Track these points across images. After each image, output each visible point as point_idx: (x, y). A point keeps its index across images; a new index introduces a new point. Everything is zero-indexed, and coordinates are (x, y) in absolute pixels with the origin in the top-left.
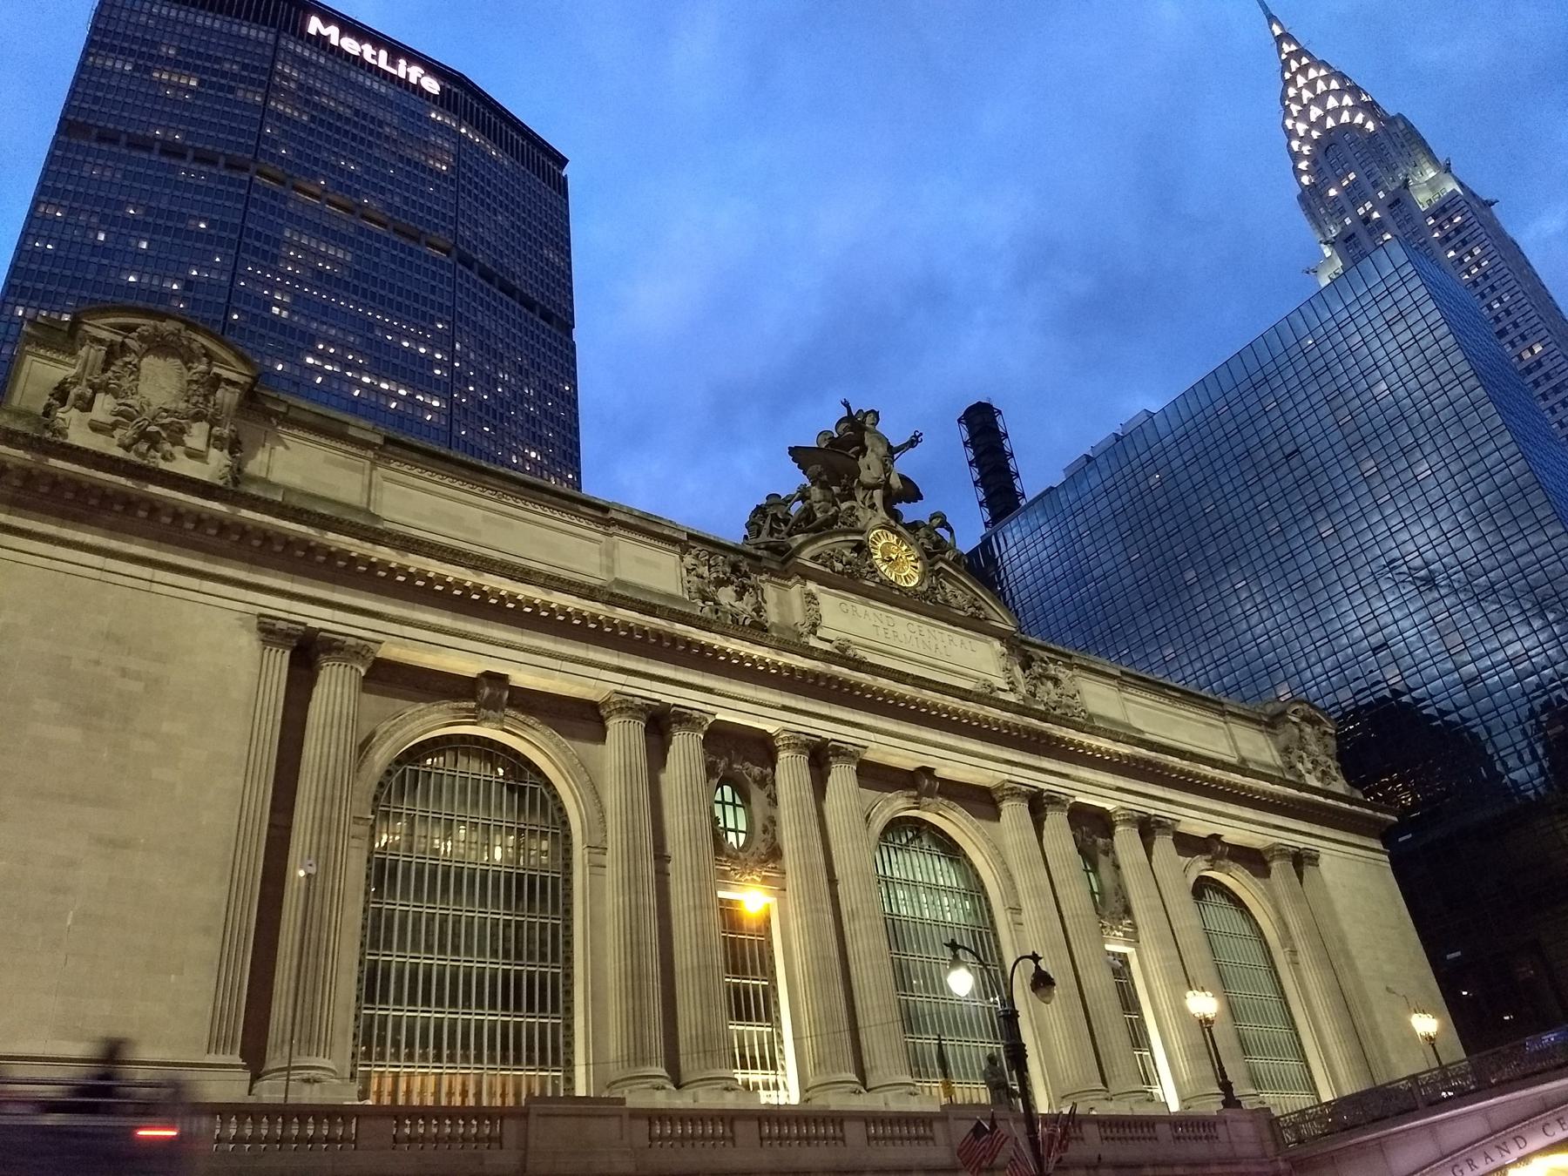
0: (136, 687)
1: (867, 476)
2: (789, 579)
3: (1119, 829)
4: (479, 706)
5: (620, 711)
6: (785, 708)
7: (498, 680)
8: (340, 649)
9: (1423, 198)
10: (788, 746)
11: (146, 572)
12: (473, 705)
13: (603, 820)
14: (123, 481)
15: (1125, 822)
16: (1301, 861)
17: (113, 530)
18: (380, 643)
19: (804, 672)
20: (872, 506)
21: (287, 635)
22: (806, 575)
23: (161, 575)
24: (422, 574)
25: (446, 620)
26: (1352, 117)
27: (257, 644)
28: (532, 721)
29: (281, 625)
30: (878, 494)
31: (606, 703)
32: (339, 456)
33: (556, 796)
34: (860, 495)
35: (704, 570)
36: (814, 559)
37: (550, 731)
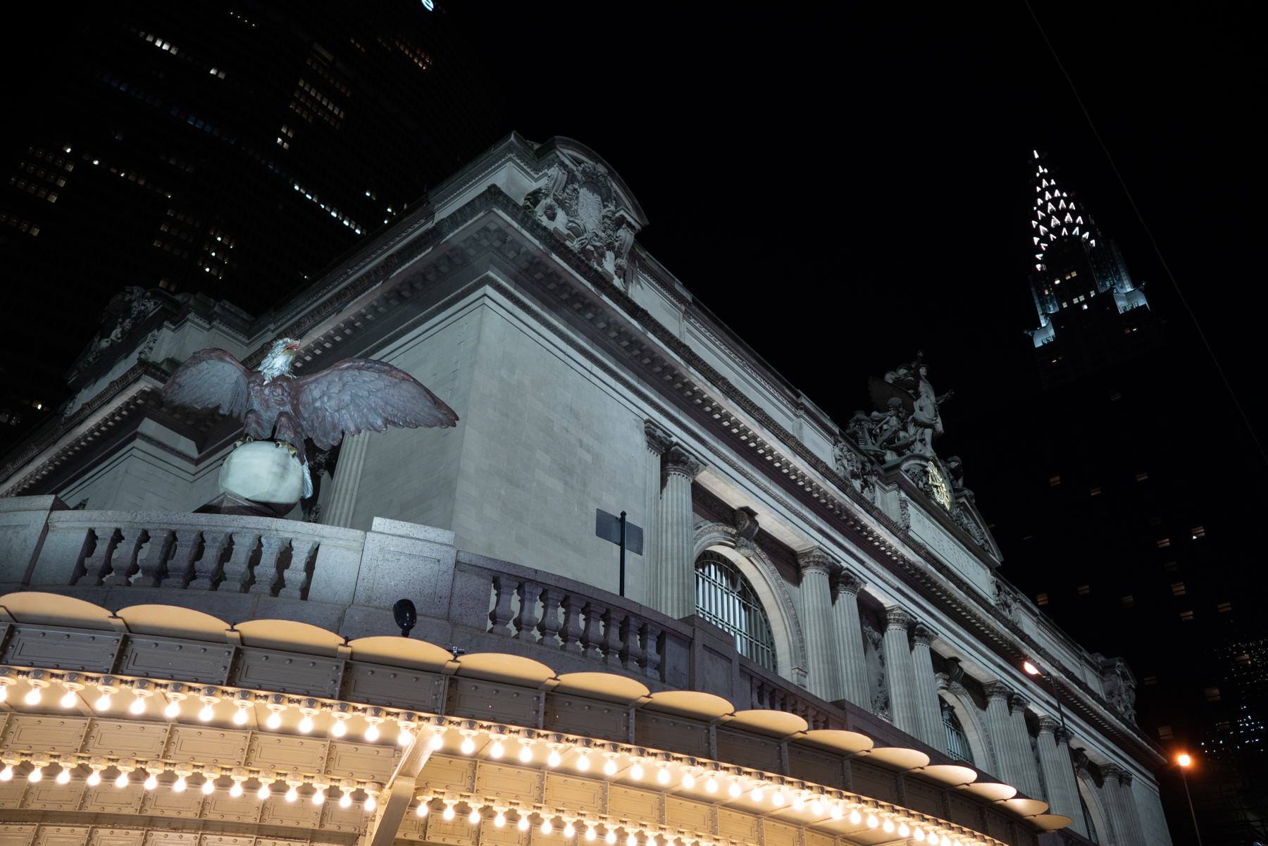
0: (588, 458)
1: (918, 414)
2: (887, 484)
3: (1043, 732)
4: (739, 535)
5: (817, 564)
6: (898, 590)
7: (750, 513)
8: (685, 463)
9: (1122, 305)
10: (898, 621)
11: (588, 364)
12: (734, 531)
13: (803, 649)
14: (589, 285)
15: (1049, 728)
16: (1124, 779)
17: (570, 322)
18: (705, 465)
19: (912, 565)
20: (922, 440)
21: (661, 443)
22: (902, 486)
23: (596, 370)
24: (727, 416)
25: (733, 457)
26: (1082, 232)
27: (645, 444)
28: (764, 556)
29: (659, 433)
30: (928, 432)
31: (806, 554)
32: (667, 304)
33: (766, 621)
34: (912, 429)
35: (845, 462)
36: (907, 471)
37: (773, 567)
